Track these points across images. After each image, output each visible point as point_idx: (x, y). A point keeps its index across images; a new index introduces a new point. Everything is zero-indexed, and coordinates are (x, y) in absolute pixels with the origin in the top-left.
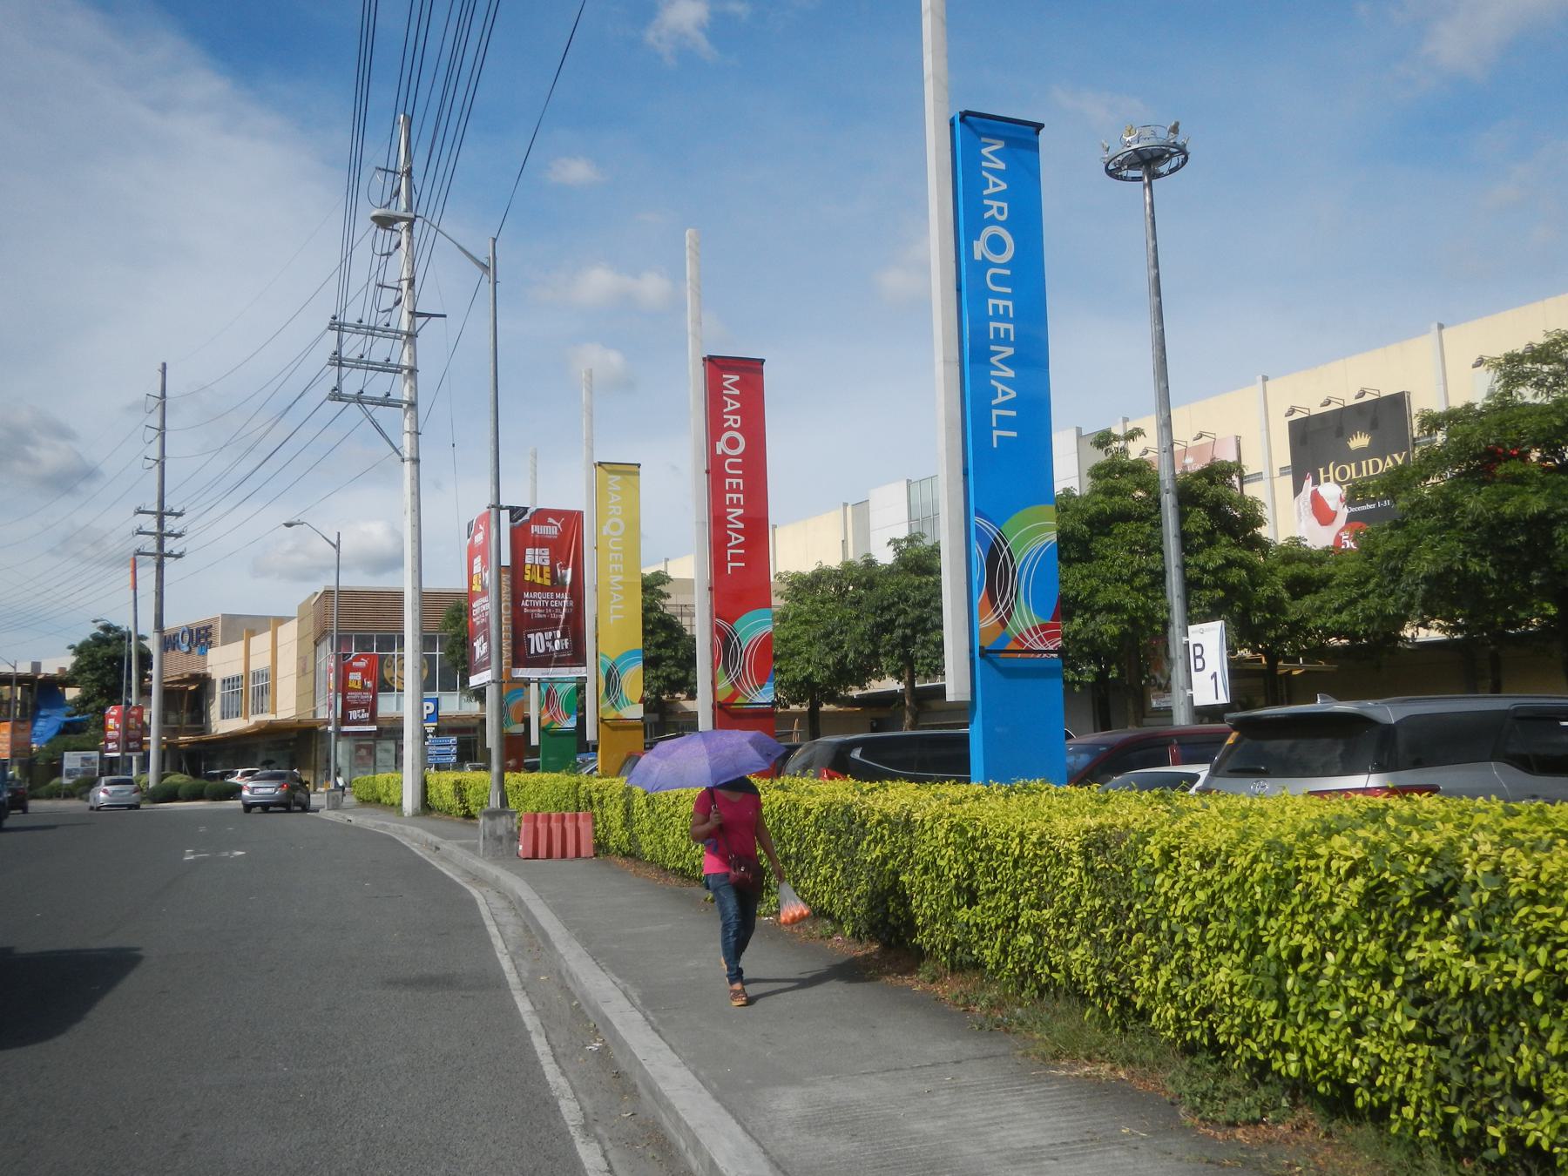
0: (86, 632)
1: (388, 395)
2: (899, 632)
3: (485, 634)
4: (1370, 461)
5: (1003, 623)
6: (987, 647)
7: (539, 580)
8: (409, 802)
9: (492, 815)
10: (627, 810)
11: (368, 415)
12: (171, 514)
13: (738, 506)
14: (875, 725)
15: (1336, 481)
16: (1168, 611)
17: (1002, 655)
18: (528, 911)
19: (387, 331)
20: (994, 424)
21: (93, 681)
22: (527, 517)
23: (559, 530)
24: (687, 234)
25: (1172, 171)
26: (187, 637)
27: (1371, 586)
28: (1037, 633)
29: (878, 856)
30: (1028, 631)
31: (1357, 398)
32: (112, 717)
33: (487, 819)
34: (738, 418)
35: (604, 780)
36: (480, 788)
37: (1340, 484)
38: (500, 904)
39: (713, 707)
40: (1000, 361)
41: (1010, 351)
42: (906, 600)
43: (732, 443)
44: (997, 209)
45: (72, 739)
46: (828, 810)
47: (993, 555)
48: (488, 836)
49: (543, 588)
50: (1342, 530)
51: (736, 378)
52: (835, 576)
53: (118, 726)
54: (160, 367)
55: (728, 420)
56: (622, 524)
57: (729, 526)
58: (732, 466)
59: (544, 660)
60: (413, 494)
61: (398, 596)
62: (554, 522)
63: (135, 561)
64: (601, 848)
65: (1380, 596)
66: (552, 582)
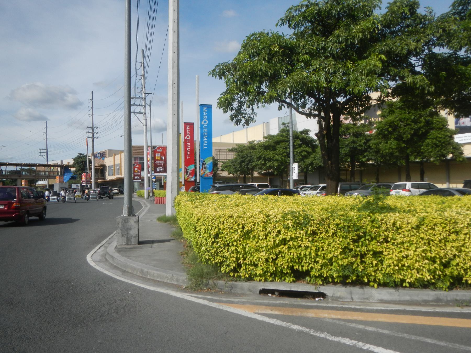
0: (76, 155)
5: (204, 172)
11: (136, 115)
16: (290, 160)
19: (139, 98)
26: (99, 155)
41: (206, 136)
44: (205, 117)
45: (73, 181)
47: (203, 164)
58: (188, 141)
59: (159, 172)
63: (87, 139)
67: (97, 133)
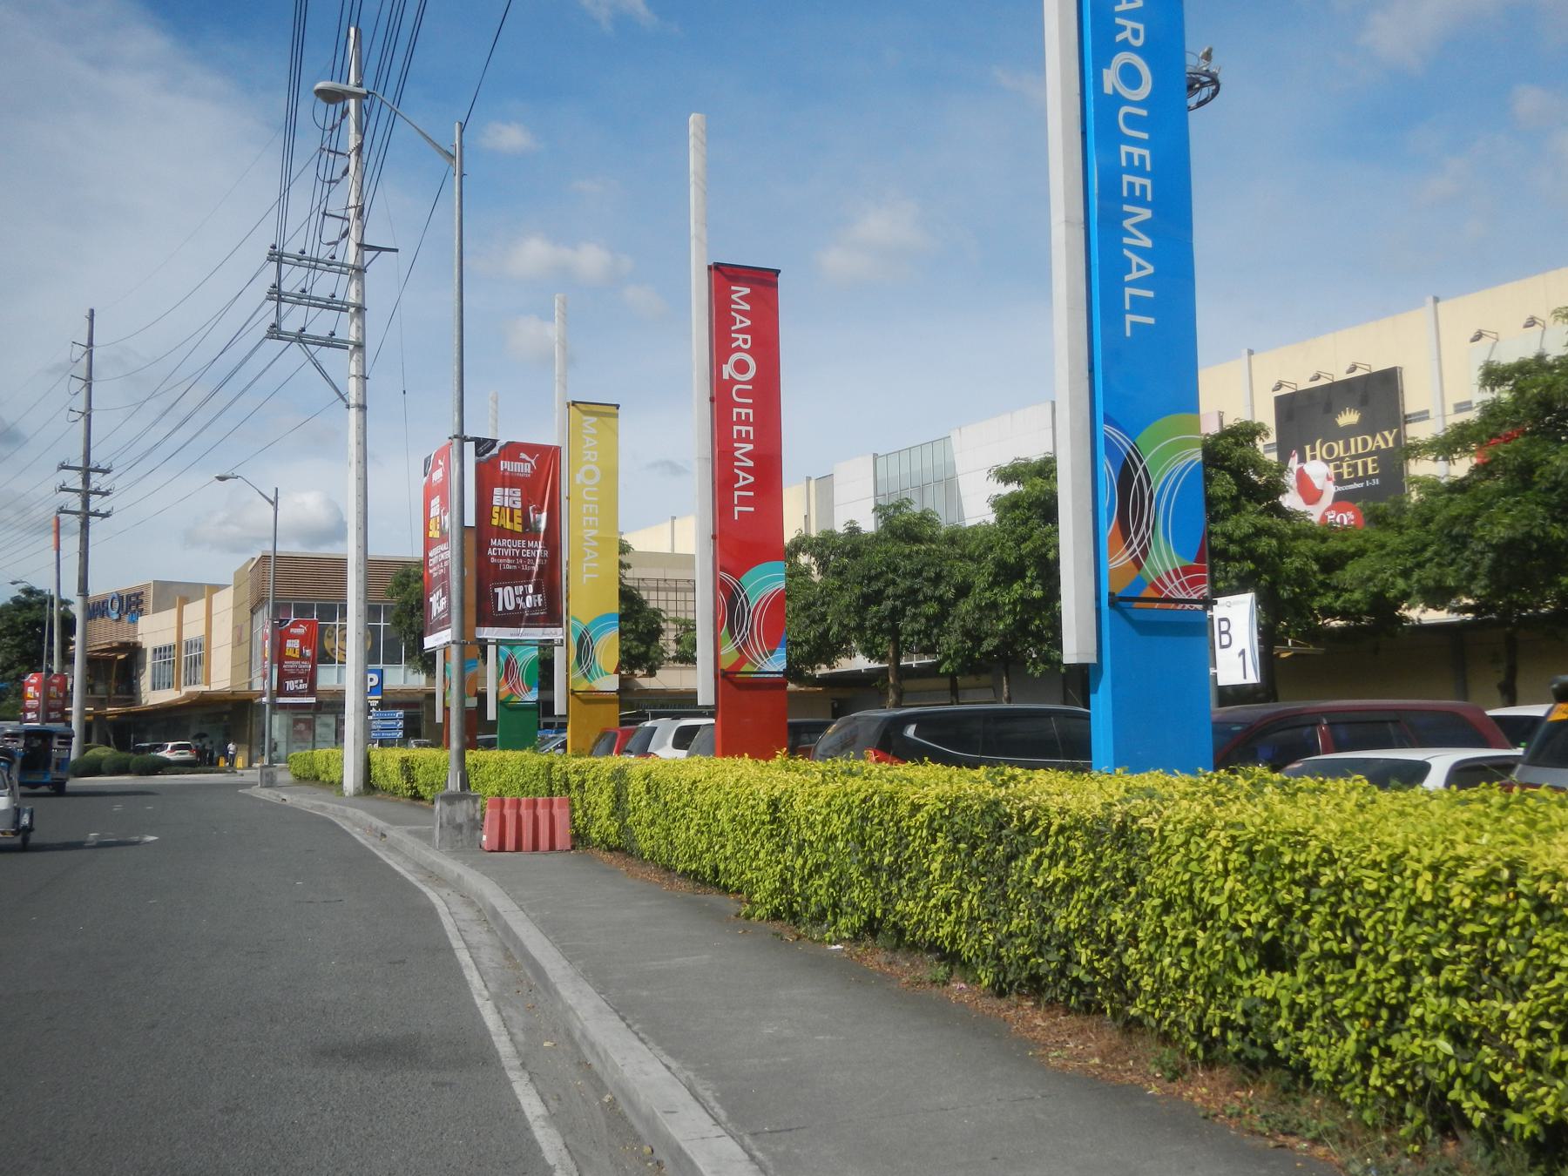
1: (333, 334)
2: (890, 603)
3: (443, 587)
4: (1359, 439)
5: (1137, 564)
6: (1118, 593)
7: (508, 526)
8: (350, 779)
9: (451, 799)
10: (618, 797)
11: (311, 357)
12: (97, 470)
13: (747, 440)
14: (836, 705)
15: (1323, 459)
17: (1136, 604)
18: (507, 929)
20: (1127, 307)
21: (13, 646)
22: (495, 451)
23: (532, 467)
24: (691, 119)
25: (1200, 104)
26: (117, 604)
27: (1428, 554)
28: (1178, 577)
29: (1057, 880)
30: (1168, 574)
31: (1349, 372)
32: (31, 685)
33: (444, 804)
34: (749, 337)
35: (584, 760)
36: (431, 766)
37: (1327, 462)
38: (466, 913)
39: (716, 677)
40: (1135, 226)
41: (1146, 214)
42: (895, 570)
43: (741, 367)
44: (1131, 31)
46: (952, 807)
48: (445, 825)
49: (512, 535)
50: (1329, 509)
51: (746, 291)
52: (817, 544)
53: (37, 694)
54: (87, 313)
55: (738, 339)
56: (597, 470)
57: (736, 464)
58: (740, 393)
59: (513, 619)
60: (358, 443)
61: (341, 564)
62: (528, 459)
64: (580, 839)
65: (1439, 565)
66: (524, 528)
67: (106, 493)
